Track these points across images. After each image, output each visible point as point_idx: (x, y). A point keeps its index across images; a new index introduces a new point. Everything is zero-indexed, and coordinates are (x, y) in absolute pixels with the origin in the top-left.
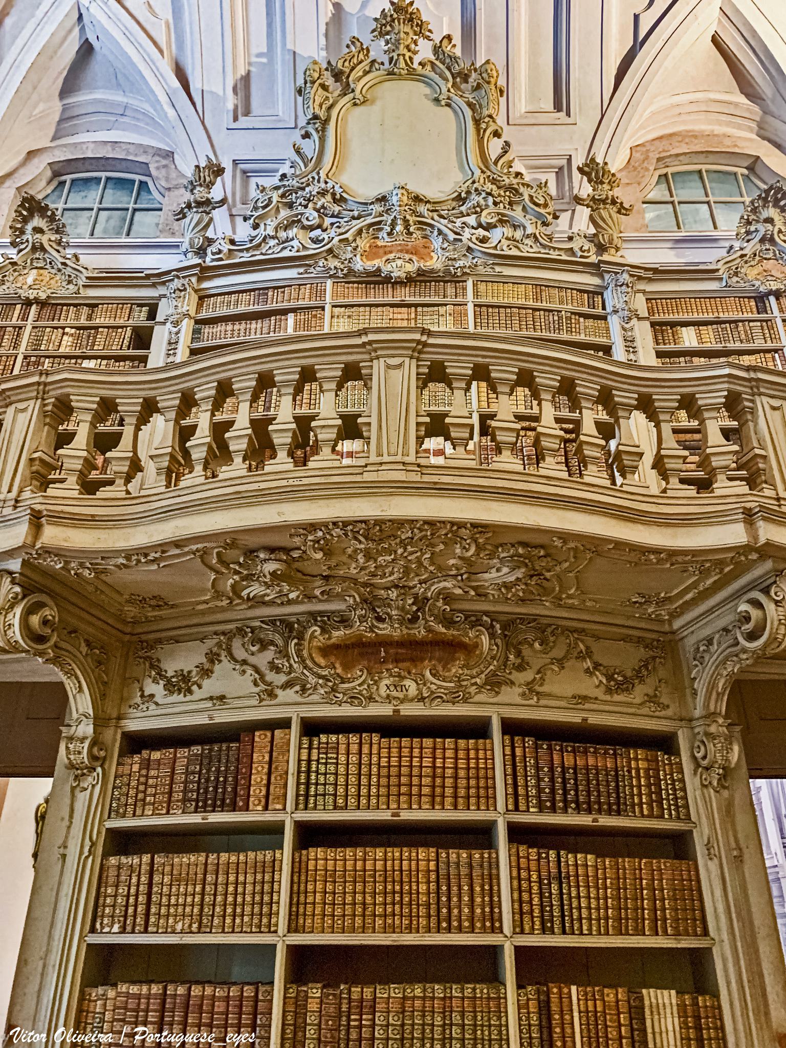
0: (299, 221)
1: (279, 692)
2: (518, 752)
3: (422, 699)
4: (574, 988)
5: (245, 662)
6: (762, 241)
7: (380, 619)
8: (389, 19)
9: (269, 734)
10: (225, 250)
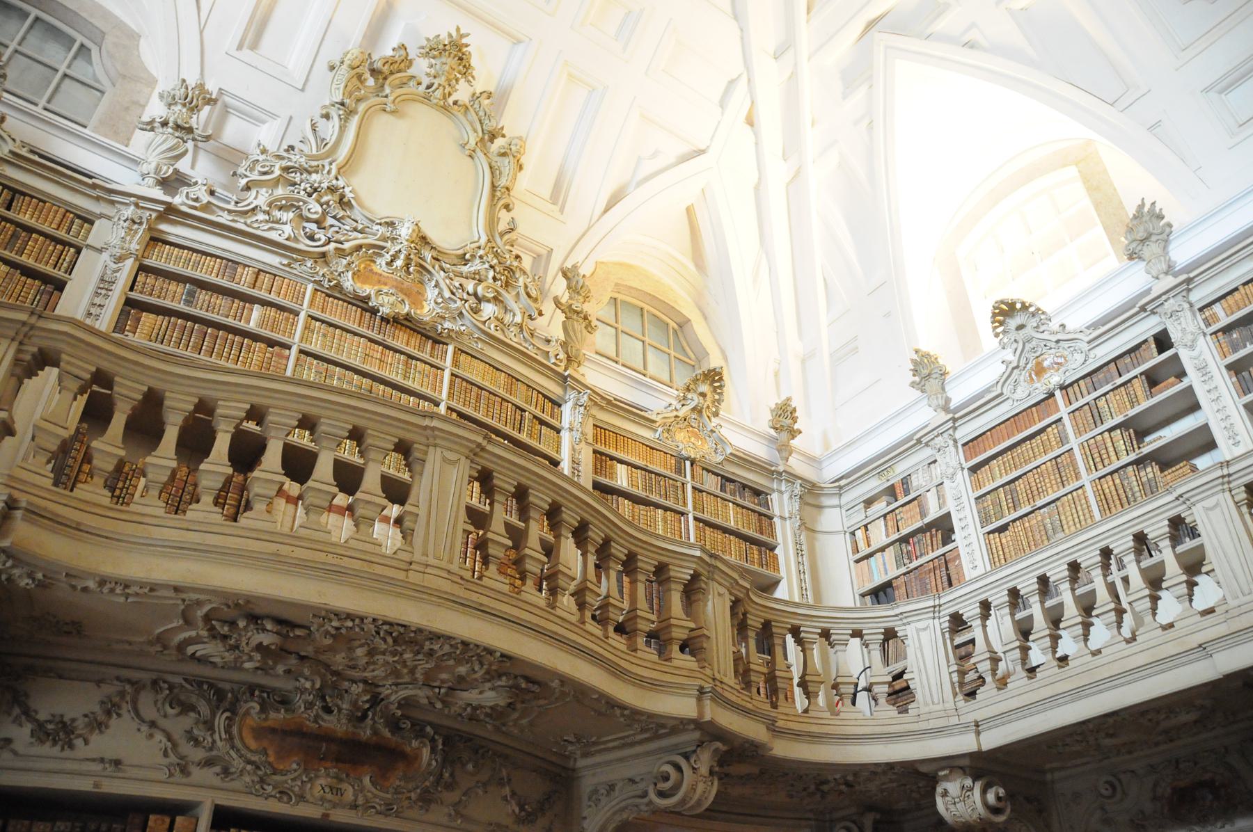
0: (298, 208)
3: (354, 806)
5: (153, 724)
6: (694, 409)
7: (328, 710)
8: (441, 47)
10: (205, 202)
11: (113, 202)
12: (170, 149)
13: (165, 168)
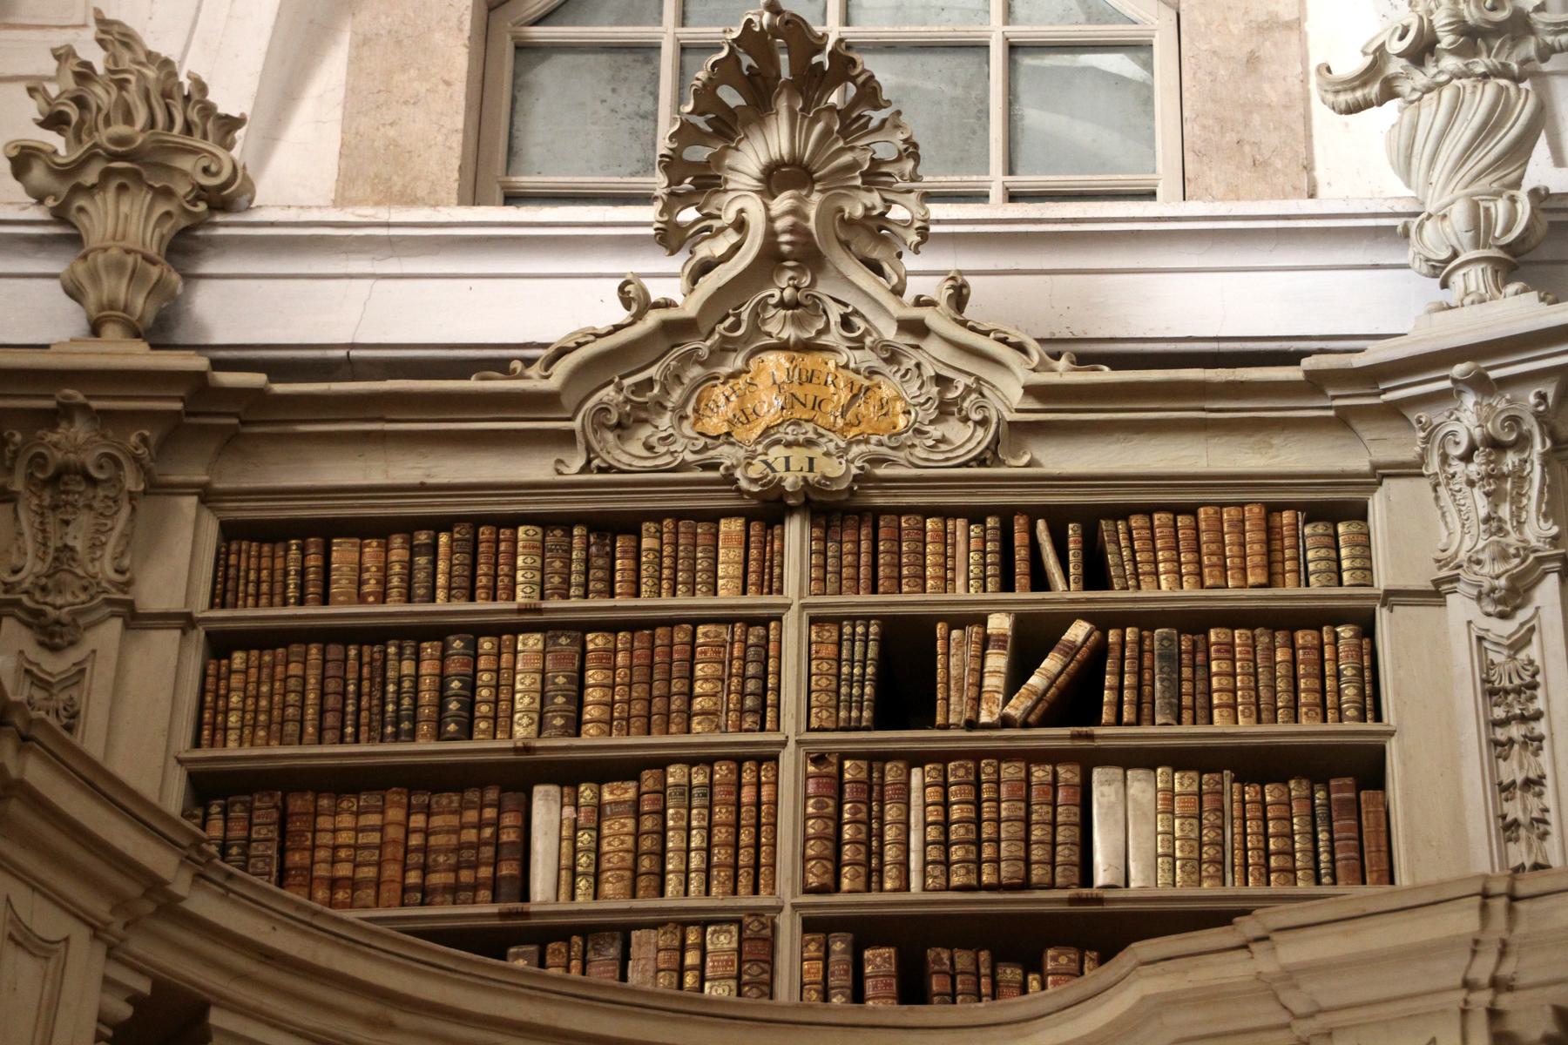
11: (1395, 412)
12: (1487, 129)
13: (1500, 208)
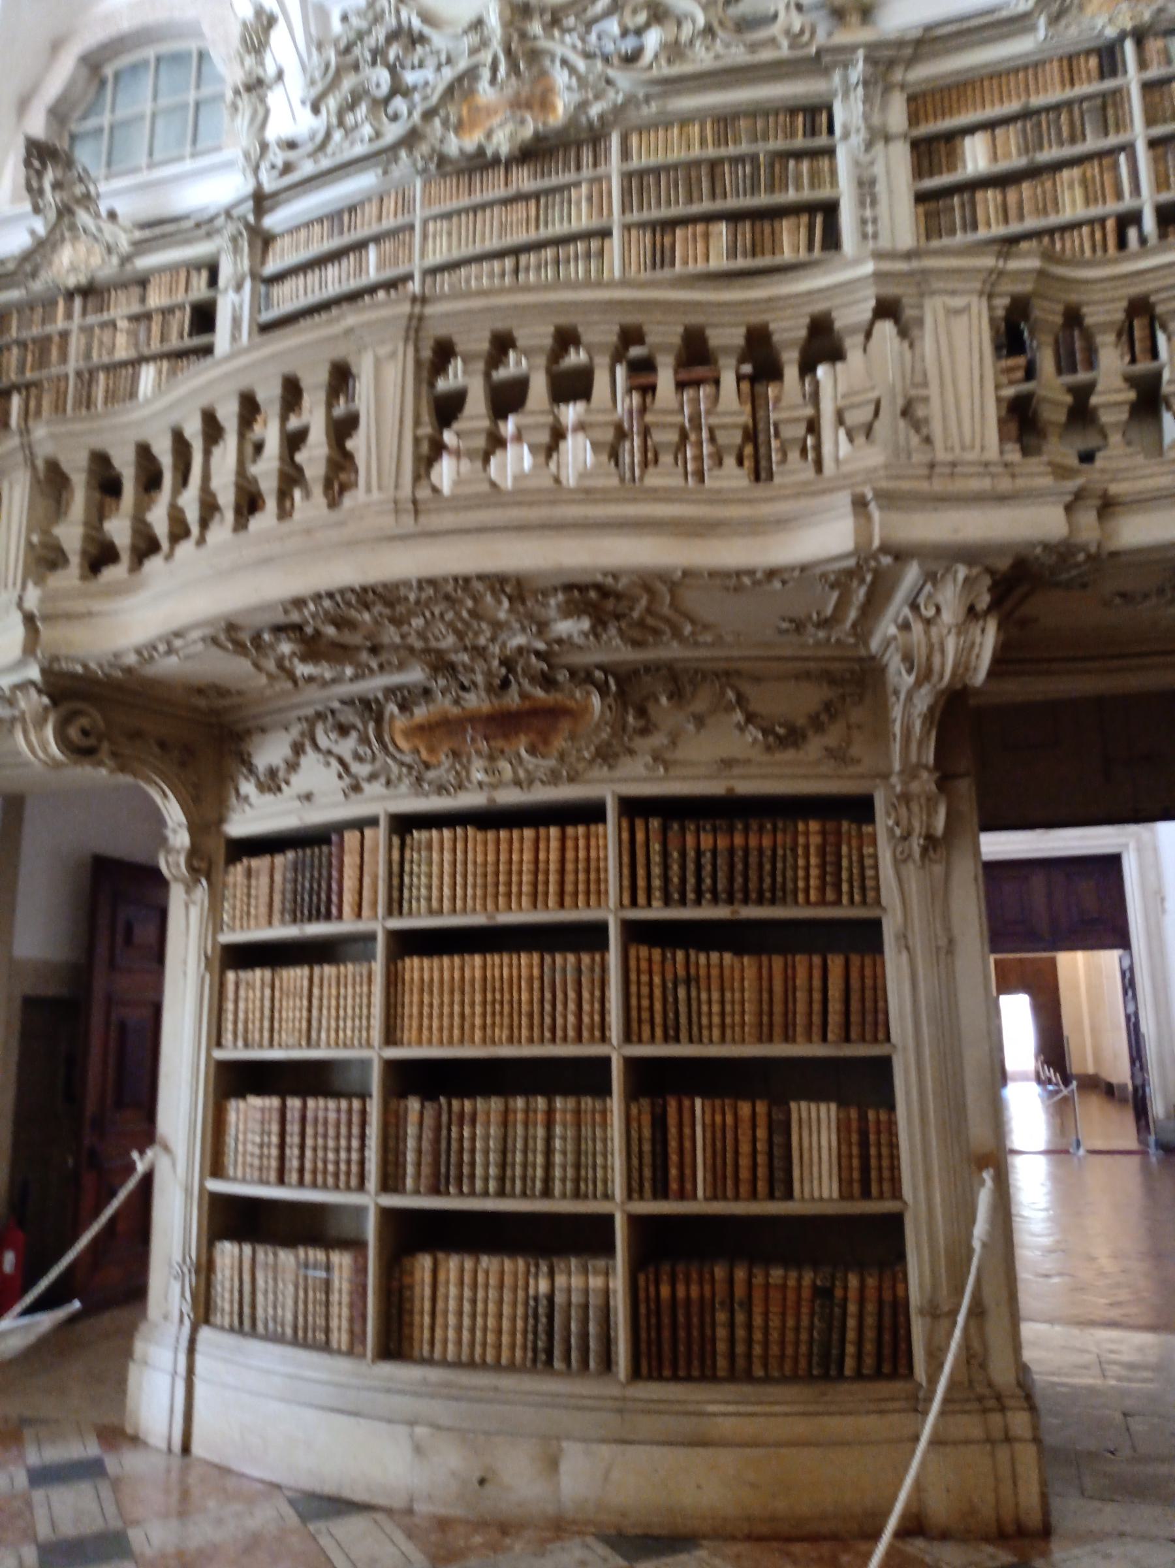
1: (365, 786)
2: (640, 837)
3: (517, 783)
4: (698, 1102)
7: (463, 688)
9: (357, 834)
